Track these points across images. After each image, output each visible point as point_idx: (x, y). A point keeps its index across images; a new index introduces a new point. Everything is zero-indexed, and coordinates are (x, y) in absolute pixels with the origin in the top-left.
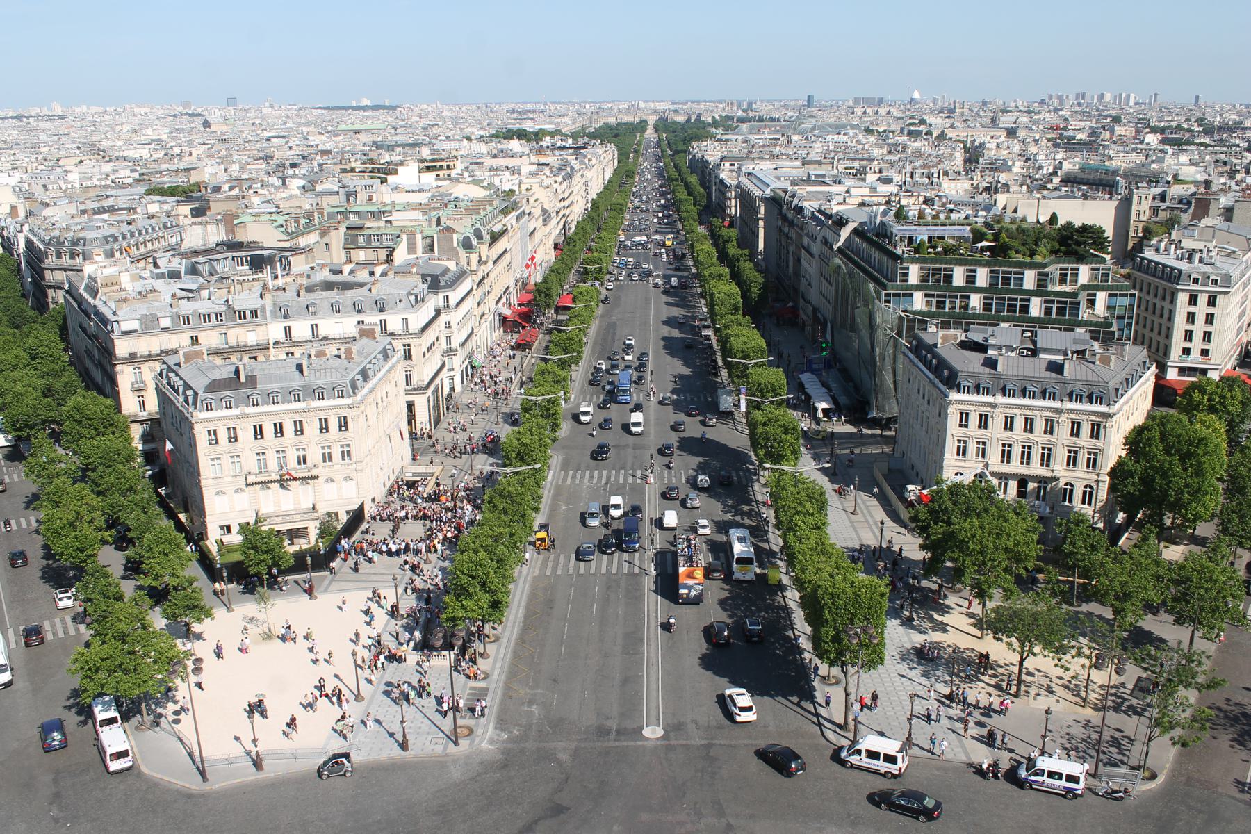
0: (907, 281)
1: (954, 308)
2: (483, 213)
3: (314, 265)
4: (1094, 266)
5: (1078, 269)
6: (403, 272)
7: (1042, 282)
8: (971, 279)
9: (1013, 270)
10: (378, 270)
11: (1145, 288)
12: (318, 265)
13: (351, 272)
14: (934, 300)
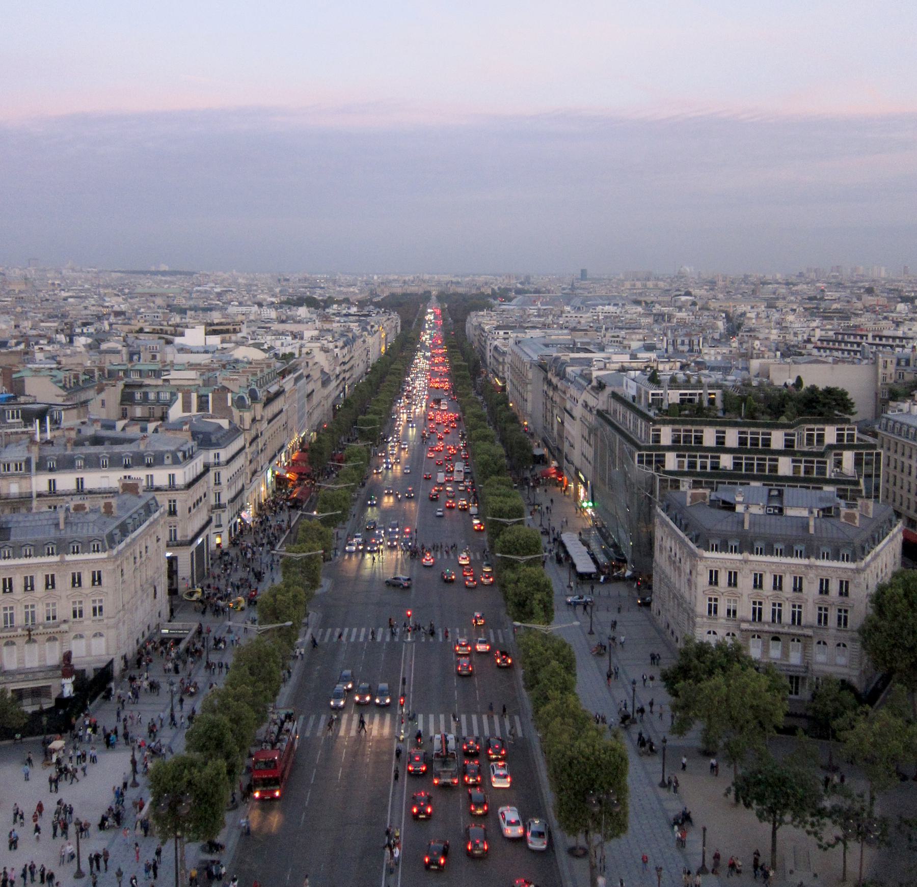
0: (659, 442)
1: (705, 467)
2: (259, 375)
3: (86, 420)
4: (840, 426)
5: (823, 430)
6: (177, 427)
7: (789, 444)
8: (720, 440)
9: (761, 430)
10: (151, 426)
11: (892, 446)
12: (90, 419)
13: (123, 429)
14: (686, 460)
